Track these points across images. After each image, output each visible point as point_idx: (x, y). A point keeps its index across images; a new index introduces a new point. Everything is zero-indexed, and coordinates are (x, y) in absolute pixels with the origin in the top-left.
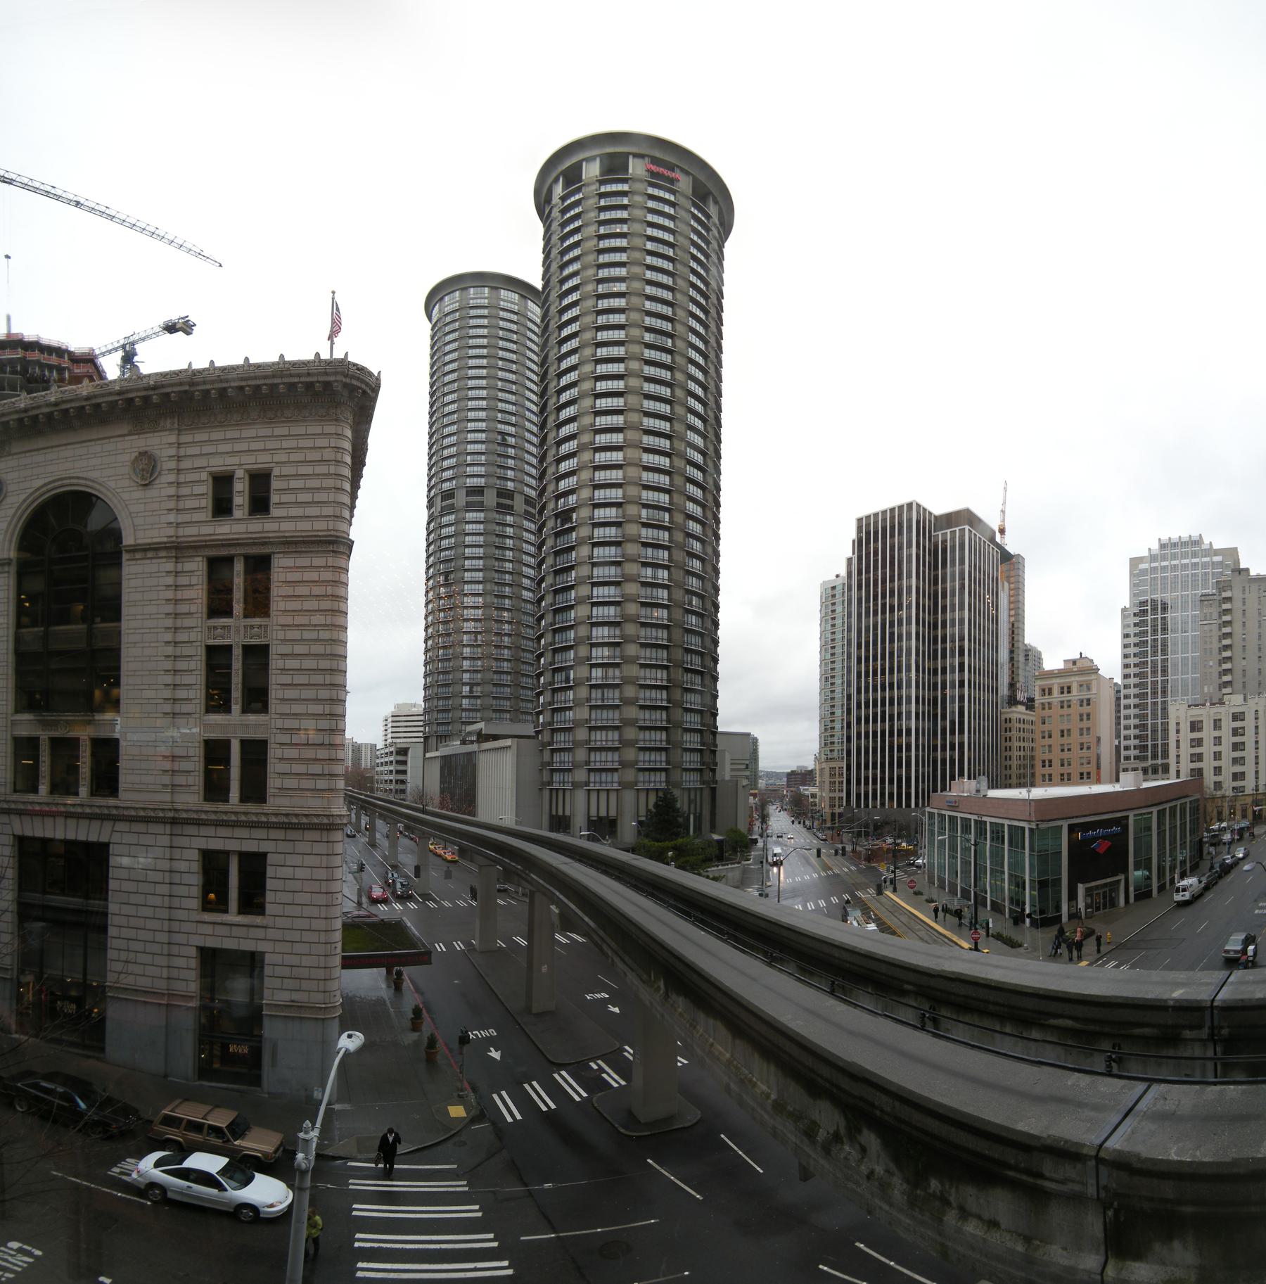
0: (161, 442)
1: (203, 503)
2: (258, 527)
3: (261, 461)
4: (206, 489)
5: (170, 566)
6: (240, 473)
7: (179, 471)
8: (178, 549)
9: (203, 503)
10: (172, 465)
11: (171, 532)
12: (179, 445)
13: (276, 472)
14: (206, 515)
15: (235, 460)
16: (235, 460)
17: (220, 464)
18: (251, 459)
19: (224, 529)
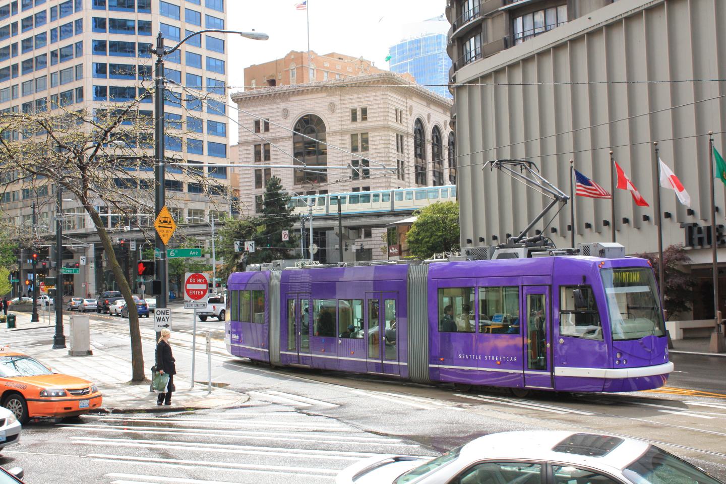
0: (335, 99)
1: (349, 118)
2: (364, 124)
3: (364, 105)
4: (349, 114)
5: (340, 138)
6: (358, 109)
7: (341, 108)
8: (342, 132)
9: (349, 118)
10: (339, 107)
11: (340, 127)
12: (341, 100)
13: (368, 108)
14: (349, 122)
15: (357, 105)
16: (357, 105)
17: (353, 106)
18: (361, 104)
19: (354, 126)
